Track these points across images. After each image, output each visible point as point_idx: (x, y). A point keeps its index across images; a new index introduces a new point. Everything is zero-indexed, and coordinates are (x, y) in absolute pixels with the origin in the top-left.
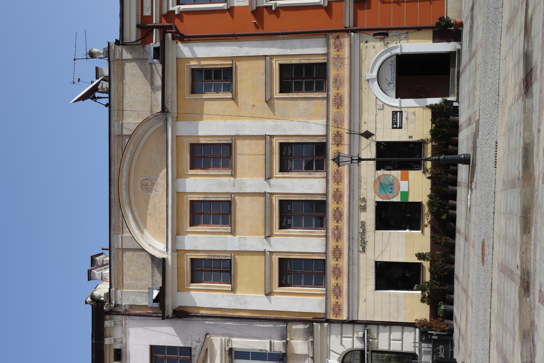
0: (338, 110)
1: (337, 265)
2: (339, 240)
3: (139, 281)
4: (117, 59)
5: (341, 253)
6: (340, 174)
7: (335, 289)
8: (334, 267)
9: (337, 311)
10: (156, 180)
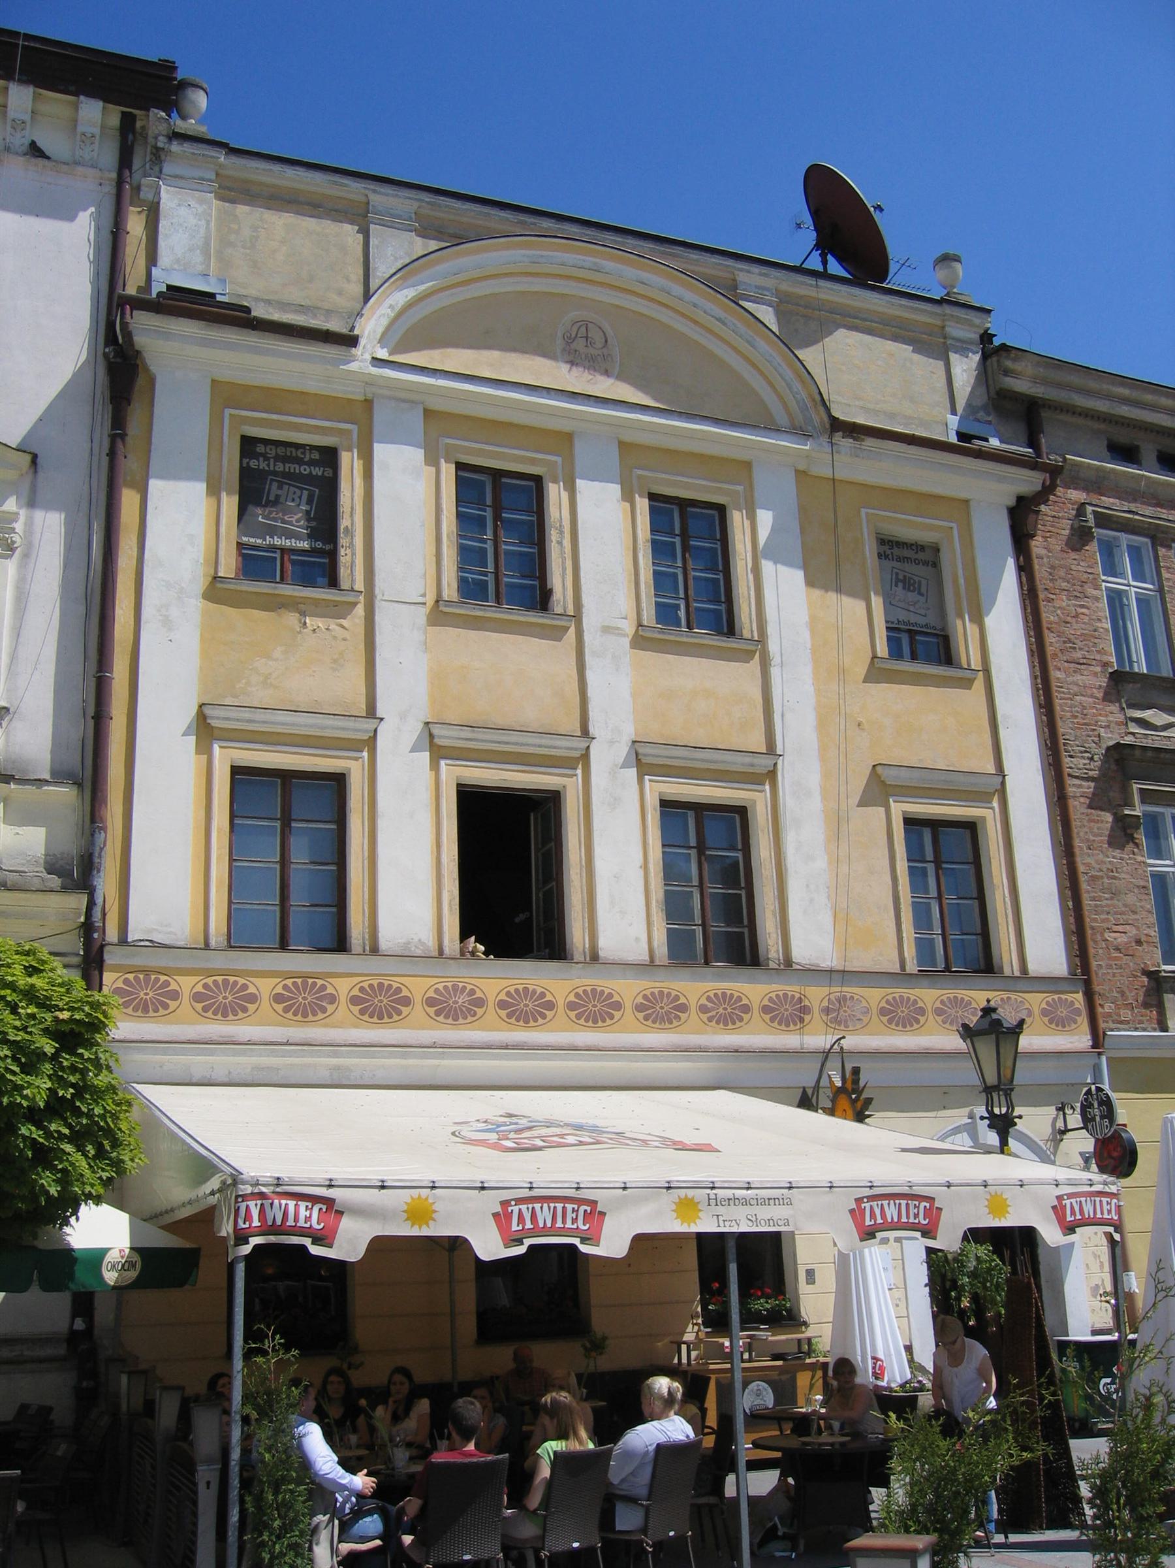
0: (875, 1011)
1: (332, 999)
3: (248, 251)
4: (943, 327)
5: (381, 1017)
9: (142, 994)
10: (607, 373)
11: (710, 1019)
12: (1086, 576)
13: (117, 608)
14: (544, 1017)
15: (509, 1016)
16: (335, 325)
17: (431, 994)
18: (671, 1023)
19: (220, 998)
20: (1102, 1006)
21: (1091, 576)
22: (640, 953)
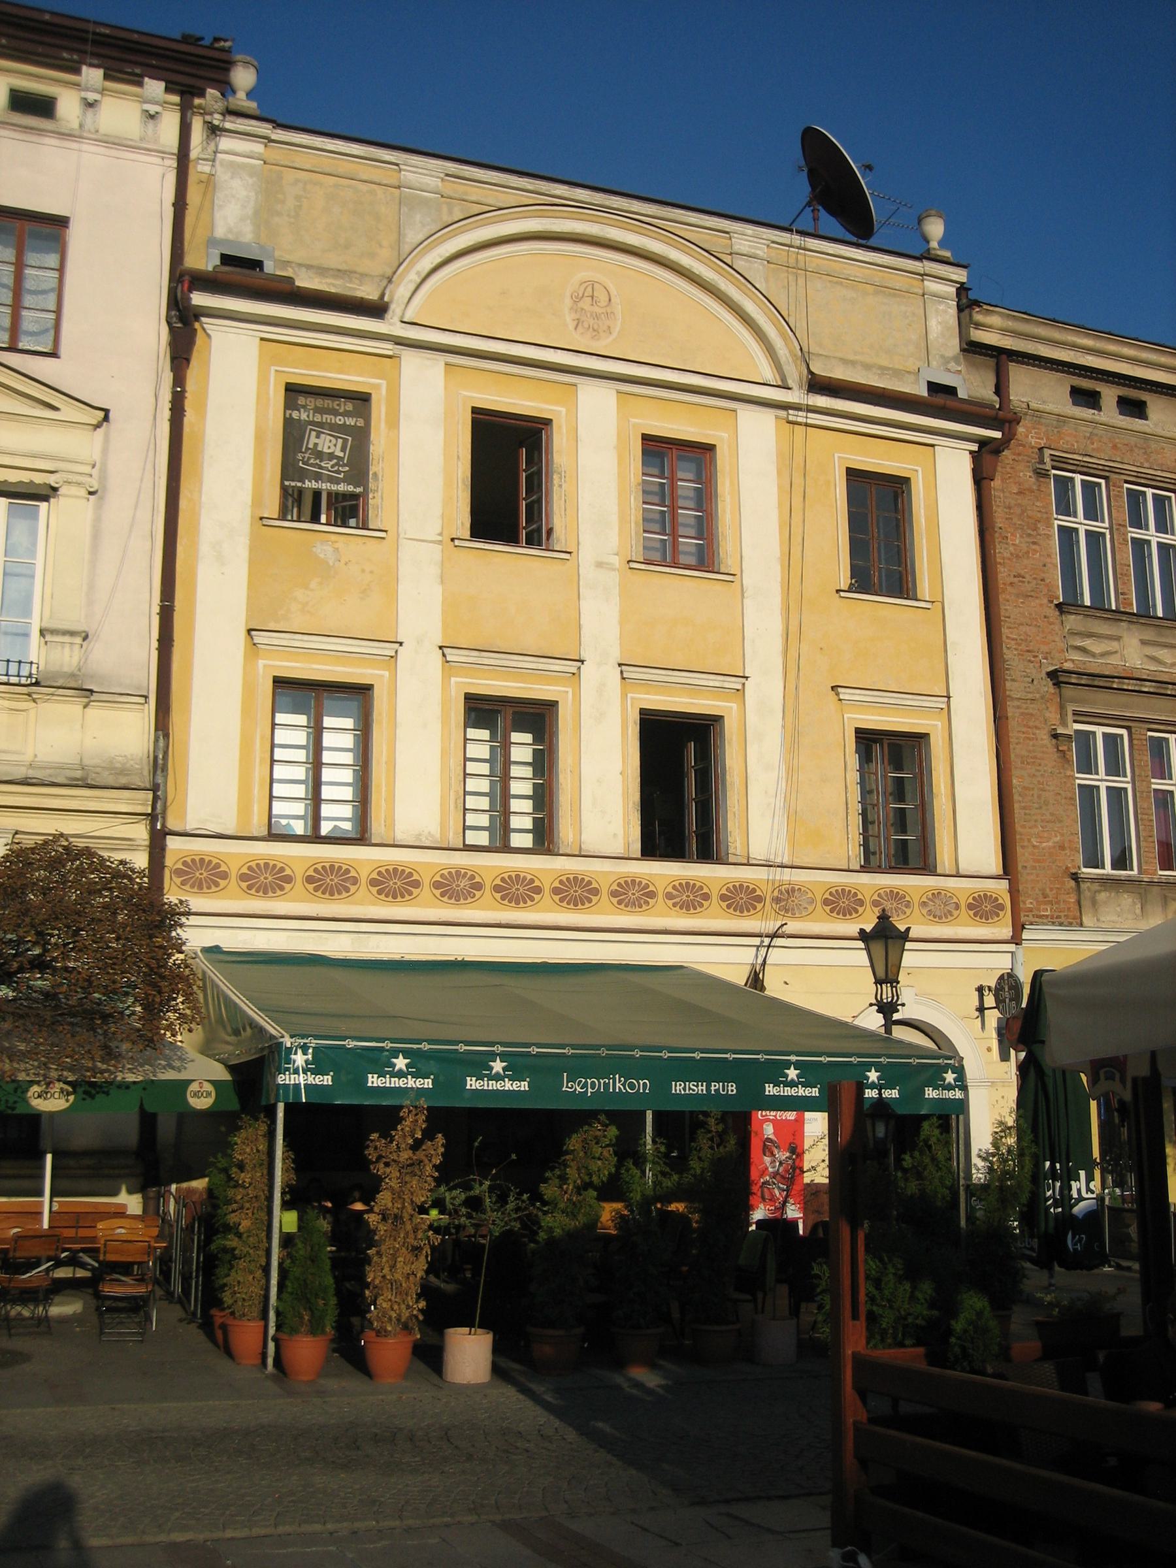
1: (355, 881)
2: (438, 892)
3: (292, 220)
5: (395, 897)
6: (642, 902)
9: (197, 874)
11: (674, 905)
12: (1039, 515)
13: (178, 545)
14: (532, 899)
15: (503, 898)
16: (368, 292)
17: (438, 878)
18: (640, 907)
19: (262, 878)
20: (1024, 903)
21: (1045, 516)
22: (618, 849)
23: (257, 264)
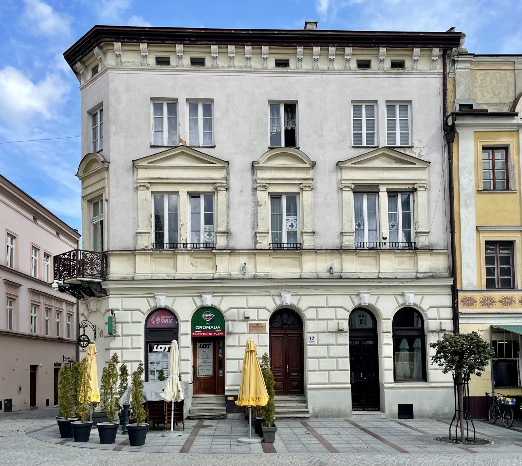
1: (515, 301)
3: (480, 88)
7: (489, 299)
8: (512, 298)
9: (468, 302)
23: (471, 106)
